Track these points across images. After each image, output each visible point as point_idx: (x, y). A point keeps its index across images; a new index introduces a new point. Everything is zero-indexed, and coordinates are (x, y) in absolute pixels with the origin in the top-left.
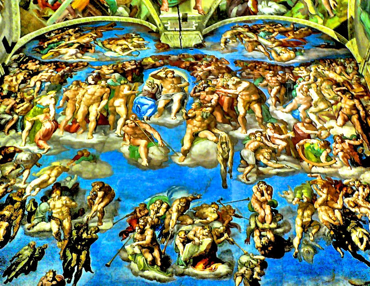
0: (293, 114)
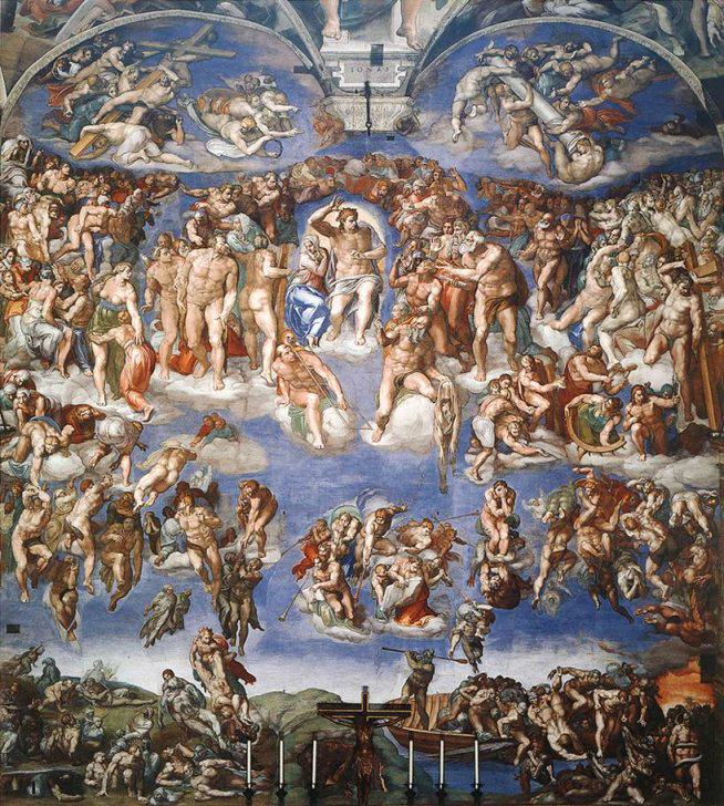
0: (571, 336)
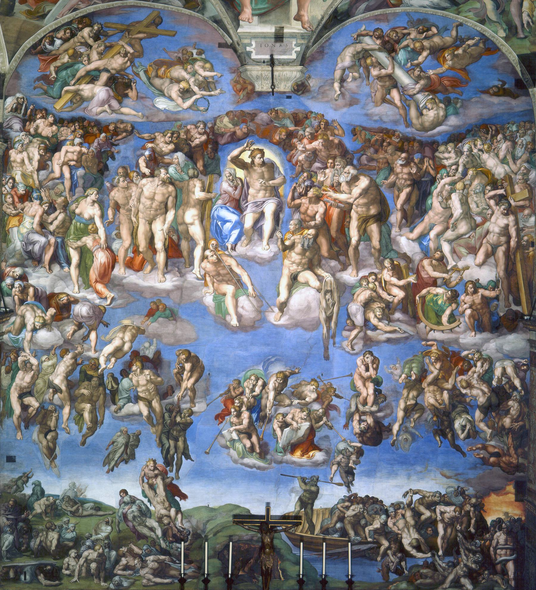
0: (421, 244)
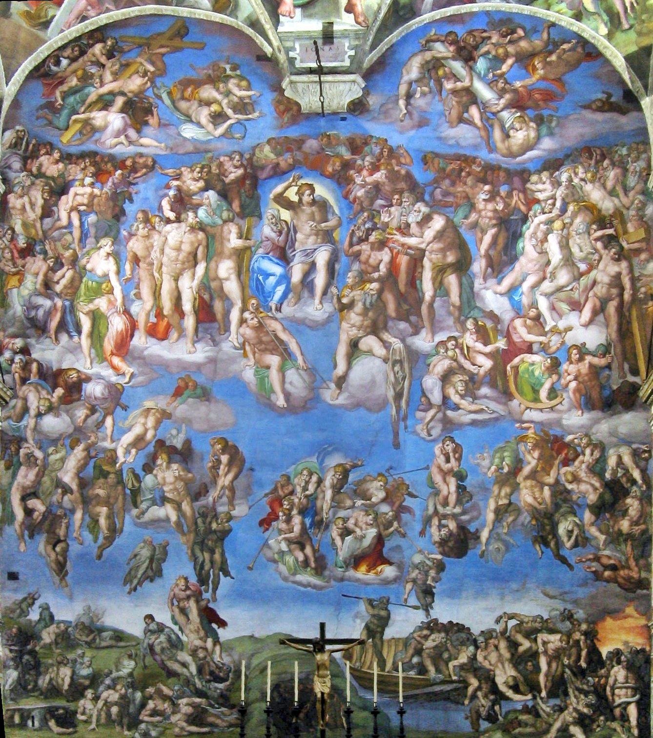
0: (511, 299)
